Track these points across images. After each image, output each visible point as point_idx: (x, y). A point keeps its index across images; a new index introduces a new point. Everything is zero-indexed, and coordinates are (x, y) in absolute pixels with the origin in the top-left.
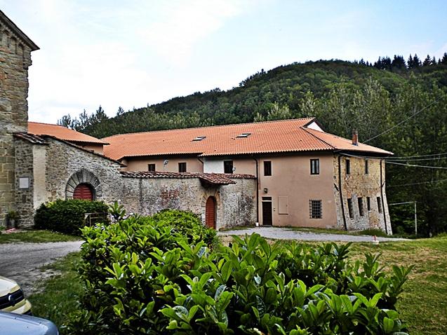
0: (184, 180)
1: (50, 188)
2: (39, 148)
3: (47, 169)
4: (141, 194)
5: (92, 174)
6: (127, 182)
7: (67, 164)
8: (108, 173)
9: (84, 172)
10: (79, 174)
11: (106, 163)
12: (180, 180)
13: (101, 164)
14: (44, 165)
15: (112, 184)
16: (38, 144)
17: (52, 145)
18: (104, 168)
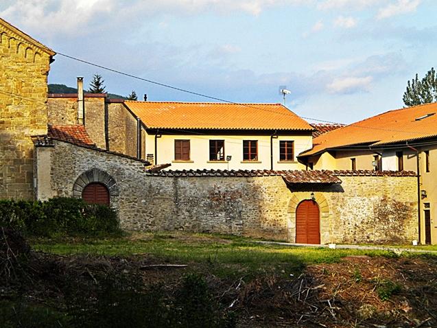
0: (250, 179)
1: (56, 187)
2: (44, 150)
3: (52, 169)
4: (176, 194)
5: (105, 173)
6: (155, 182)
7: (75, 164)
8: (127, 172)
9: (95, 172)
10: (89, 174)
11: (124, 162)
12: (244, 179)
13: (118, 163)
14: (49, 165)
15: (133, 184)
16: (41, 146)
17: (57, 147)
18: (122, 166)
